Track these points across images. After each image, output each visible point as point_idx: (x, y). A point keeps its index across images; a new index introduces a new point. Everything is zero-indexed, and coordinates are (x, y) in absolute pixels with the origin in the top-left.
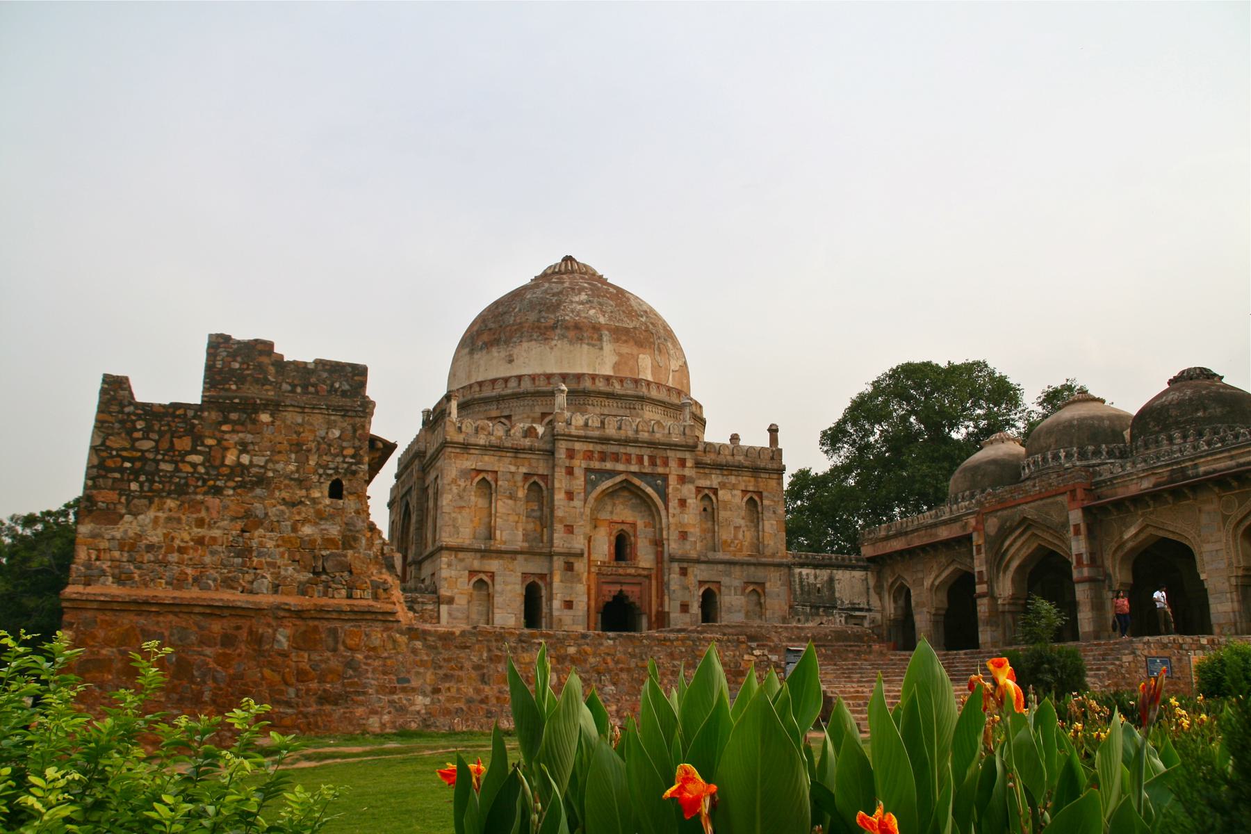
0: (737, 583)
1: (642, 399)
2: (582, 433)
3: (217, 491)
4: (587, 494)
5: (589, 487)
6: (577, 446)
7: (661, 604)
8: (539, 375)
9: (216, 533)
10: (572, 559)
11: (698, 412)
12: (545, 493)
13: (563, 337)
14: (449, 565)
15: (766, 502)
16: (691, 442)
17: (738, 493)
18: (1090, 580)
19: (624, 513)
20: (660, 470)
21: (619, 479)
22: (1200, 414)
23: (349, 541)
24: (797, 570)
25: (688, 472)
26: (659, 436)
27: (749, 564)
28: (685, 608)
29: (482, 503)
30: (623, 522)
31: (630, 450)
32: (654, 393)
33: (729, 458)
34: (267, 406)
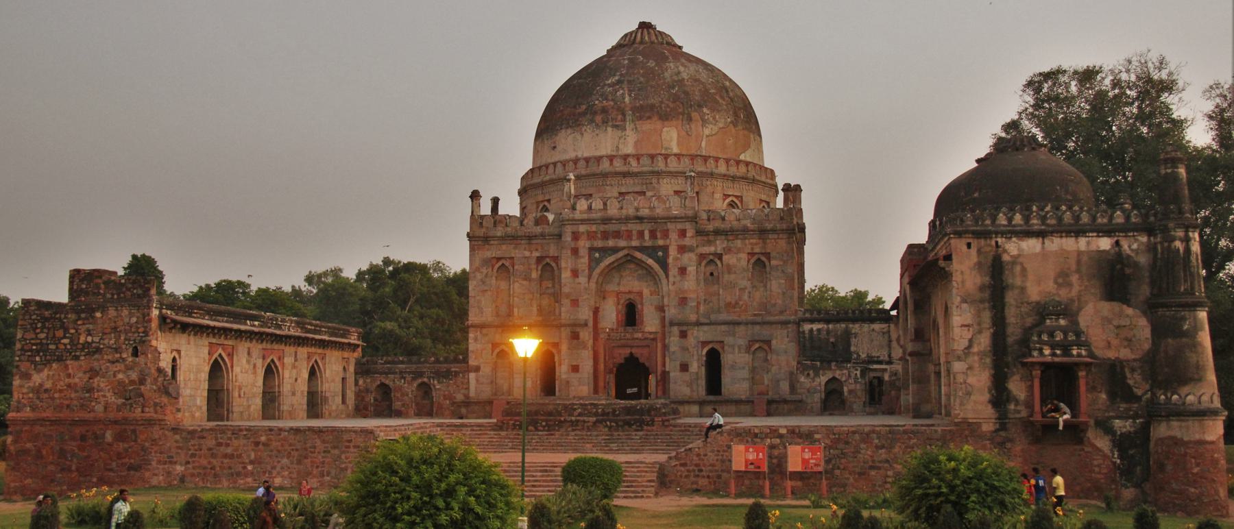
0: (742, 342)
1: (658, 174)
2: (585, 216)
3: (77, 358)
4: (591, 269)
5: (593, 264)
6: (582, 228)
7: (664, 365)
8: (568, 161)
9: (77, 380)
10: (578, 329)
11: (743, 169)
12: (556, 272)
13: (592, 121)
14: (476, 340)
15: (773, 262)
16: (690, 213)
17: (744, 256)
18: (910, 354)
19: (631, 283)
20: (661, 242)
21: (621, 254)
22: (976, 195)
23: (142, 381)
24: (807, 327)
25: (688, 241)
26: (659, 211)
27: (754, 323)
28: (684, 367)
29: (503, 285)
30: (630, 292)
31: (631, 226)
32: (673, 165)
33: (735, 223)
34: (97, 310)
